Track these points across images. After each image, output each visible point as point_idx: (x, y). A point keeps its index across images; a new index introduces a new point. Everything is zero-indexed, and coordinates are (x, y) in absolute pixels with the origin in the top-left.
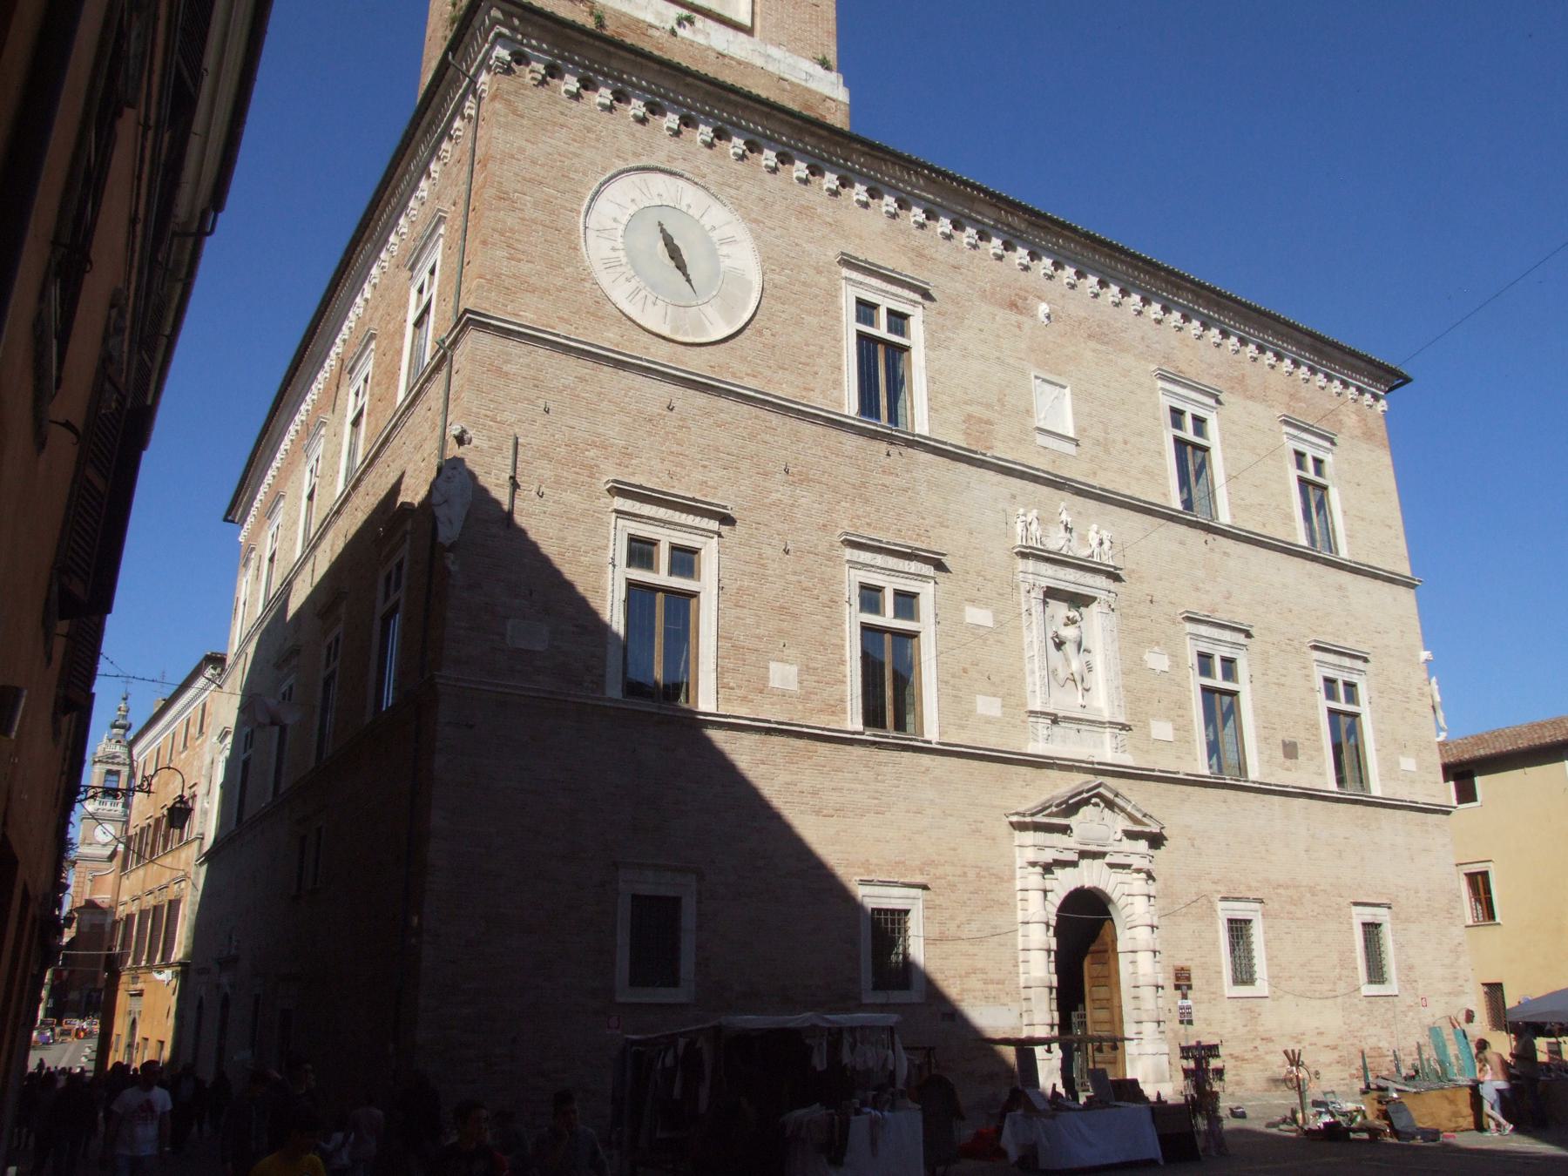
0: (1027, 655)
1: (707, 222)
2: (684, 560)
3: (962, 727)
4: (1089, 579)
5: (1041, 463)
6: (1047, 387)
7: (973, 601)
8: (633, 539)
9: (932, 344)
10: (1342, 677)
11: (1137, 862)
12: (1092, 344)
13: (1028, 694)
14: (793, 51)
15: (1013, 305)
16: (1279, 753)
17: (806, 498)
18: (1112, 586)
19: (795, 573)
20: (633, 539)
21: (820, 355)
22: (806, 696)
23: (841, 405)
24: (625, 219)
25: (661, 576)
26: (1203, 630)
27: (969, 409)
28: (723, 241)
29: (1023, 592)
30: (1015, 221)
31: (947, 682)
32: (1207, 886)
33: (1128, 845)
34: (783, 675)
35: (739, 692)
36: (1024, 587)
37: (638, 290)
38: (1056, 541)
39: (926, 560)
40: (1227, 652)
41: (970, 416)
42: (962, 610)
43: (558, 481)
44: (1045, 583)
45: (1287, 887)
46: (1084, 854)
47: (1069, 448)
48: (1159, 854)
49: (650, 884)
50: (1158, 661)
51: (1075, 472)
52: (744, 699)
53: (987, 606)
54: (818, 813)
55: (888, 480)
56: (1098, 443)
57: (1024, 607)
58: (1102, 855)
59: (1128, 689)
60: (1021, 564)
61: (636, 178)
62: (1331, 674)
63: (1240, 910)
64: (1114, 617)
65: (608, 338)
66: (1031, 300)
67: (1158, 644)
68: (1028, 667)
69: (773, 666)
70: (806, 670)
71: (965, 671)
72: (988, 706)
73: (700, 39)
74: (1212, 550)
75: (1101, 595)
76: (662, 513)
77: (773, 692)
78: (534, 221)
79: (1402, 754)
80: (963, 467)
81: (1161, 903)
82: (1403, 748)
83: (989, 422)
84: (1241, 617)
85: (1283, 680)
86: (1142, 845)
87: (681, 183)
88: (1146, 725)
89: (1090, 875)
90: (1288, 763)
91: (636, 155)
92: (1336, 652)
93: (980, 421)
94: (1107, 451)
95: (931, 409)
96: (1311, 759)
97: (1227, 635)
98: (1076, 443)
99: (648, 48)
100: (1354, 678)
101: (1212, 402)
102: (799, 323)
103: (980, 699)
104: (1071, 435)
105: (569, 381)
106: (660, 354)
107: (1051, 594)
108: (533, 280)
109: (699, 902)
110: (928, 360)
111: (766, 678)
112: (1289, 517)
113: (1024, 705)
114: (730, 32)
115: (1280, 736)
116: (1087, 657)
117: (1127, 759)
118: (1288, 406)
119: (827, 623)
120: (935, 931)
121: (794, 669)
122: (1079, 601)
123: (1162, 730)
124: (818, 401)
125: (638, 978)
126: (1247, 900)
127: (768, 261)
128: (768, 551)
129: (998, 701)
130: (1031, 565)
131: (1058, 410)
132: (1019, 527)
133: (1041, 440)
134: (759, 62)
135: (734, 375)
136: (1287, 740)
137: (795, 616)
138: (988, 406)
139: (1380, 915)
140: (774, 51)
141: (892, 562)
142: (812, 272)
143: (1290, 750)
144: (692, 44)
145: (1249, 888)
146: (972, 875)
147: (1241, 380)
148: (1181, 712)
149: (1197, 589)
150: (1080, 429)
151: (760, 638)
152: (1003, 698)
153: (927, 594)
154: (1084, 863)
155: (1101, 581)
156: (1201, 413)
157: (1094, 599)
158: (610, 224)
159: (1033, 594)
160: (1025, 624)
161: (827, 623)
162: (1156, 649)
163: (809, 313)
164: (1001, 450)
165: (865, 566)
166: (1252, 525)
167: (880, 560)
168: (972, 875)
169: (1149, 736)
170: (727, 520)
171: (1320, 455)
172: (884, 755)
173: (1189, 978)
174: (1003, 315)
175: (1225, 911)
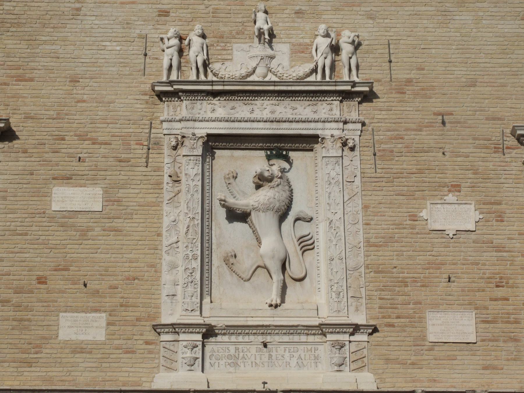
0: (167, 240)
7: (67, 179)
13: (164, 298)
18: (352, 110)
29: (166, 150)
36: (169, 142)
42: (48, 195)
50: (453, 216)
53: (94, 181)
57: (167, 171)
60: (166, 110)
64: (354, 162)
67: (456, 188)
71: (42, 280)
72: (81, 327)
88: (417, 320)
113: (157, 315)
116: (303, 229)
122: (280, 146)
129: (102, 318)
130: (183, 108)
148: (500, 292)
152: (110, 315)
157: (314, 139)
159: (183, 151)
160: (167, 196)
162: (451, 198)
169: (424, 338)
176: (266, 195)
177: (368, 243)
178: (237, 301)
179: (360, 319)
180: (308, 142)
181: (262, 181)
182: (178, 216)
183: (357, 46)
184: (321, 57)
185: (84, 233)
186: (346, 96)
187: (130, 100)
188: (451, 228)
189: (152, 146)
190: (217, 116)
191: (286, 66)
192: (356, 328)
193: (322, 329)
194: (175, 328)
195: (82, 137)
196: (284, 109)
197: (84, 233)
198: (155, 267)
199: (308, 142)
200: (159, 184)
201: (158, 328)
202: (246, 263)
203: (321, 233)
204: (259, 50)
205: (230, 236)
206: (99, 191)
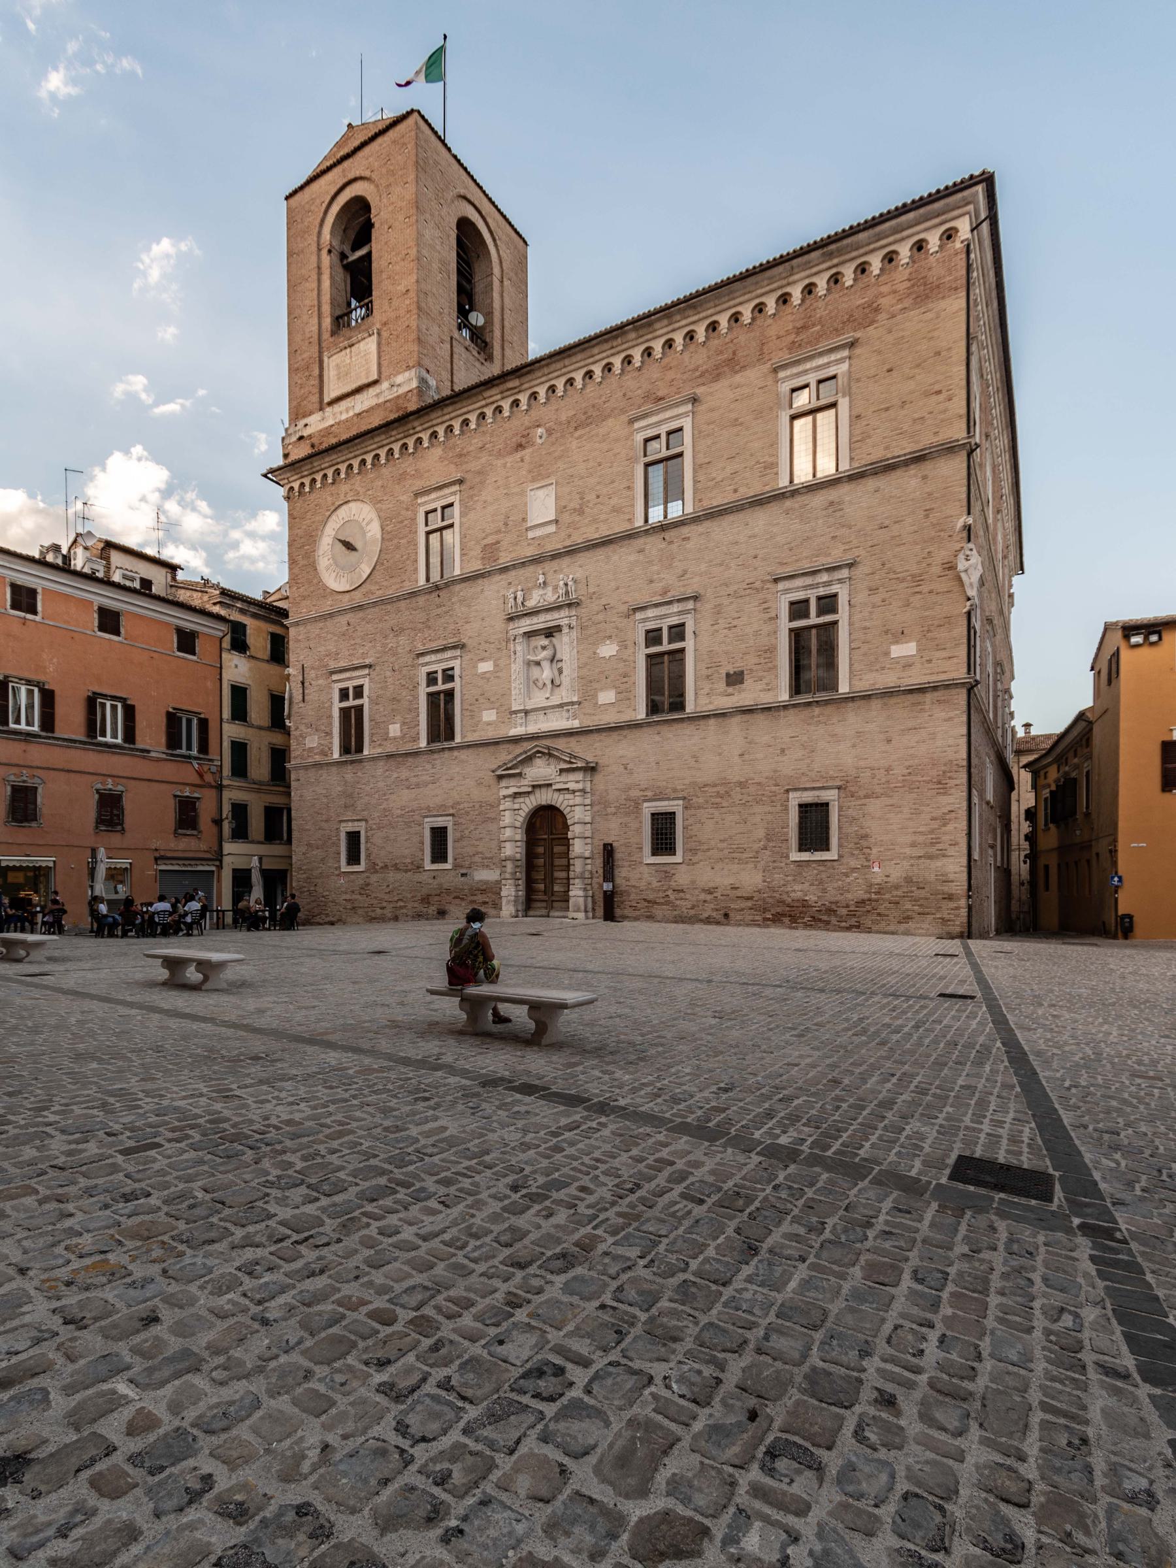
4: (556, 615)
5: (530, 552)
7: (482, 660)
11: (572, 786)
15: (520, 446)
16: (722, 685)
17: (403, 640)
22: (403, 737)
26: (650, 613)
32: (635, 793)
33: (564, 778)
34: (395, 730)
39: (454, 648)
40: (675, 621)
44: (522, 630)
45: (715, 785)
47: (552, 529)
48: (598, 778)
50: (608, 650)
55: (439, 611)
60: (511, 625)
61: (334, 517)
64: (574, 634)
72: (489, 716)
74: (671, 542)
76: (347, 675)
79: (897, 642)
80: (480, 581)
81: (596, 808)
82: (901, 636)
85: (735, 623)
88: (595, 696)
89: (543, 798)
90: (730, 690)
97: (675, 608)
100: (835, 589)
107: (529, 635)
117: (576, 724)
120: (458, 835)
122: (550, 633)
126: (669, 799)
130: (516, 624)
133: (531, 535)
141: (439, 656)
145: (675, 790)
149: (652, 581)
154: (537, 791)
164: (505, 559)
167: (433, 657)
170: (370, 666)
172: (436, 756)
175: (648, 808)
176: (545, 654)
178: (539, 699)
180: (558, 628)
181: (544, 648)
182: (517, 667)
183: (575, 581)
184: (561, 591)
186: (570, 605)
187: (500, 624)
188: (607, 655)
189: (508, 641)
190: (526, 625)
191: (550, 597)
192: (572, 703)
193: (561, 706)
194: (515, 712)
196: (549, 616)
199: (558, 628)
202: (540, 684)
203: (565, 666)
204: (541, 592)
205: (535, 672)
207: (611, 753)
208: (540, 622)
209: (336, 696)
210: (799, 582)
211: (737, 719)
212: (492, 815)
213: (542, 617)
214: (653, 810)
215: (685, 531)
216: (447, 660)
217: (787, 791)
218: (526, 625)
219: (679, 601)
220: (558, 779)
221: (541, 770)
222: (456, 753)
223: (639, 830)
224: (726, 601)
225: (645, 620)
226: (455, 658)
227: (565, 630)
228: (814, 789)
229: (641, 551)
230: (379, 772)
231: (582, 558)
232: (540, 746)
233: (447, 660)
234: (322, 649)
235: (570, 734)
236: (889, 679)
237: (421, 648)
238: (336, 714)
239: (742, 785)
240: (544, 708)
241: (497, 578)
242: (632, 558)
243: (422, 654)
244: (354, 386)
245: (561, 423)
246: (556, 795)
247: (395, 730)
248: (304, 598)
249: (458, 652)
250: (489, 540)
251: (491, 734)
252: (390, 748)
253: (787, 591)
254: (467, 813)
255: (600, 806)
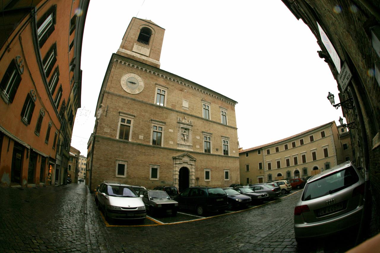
1: (138, 79)
2: (129, 122)
3: (167, 145)
4: (188, 126)
5: (183, 111)
6: (185, 101)
7: (170, 129)
8: (122, 119)
9: (168, 95)
10: (226, 140)
12: (192, 96)
14: (154, 59)
15: (181, 90)
16: (215, 150)
17: (147, 114)
19: (144, 124)
20: (122, 119)
21: (151, 96)
23: (154, 102)
24: (127, 79)
25: (126, 124)
26: (205, 134)
27: (173, 103)
28: (140, 81)
30: (182, 80)
31: (165, 139)
32: (203, 167)
33: (191, 162)
34: (141, 137)
35: (135, 139)
37: (127, 88)
38: (183, 121)
40: (209, 137)
41: (172, 104)
43: (113, 111)
44: (181, 126)
46: (184, 162)
47: (188, 109)
48: (196, 163)
49: (121, 163)
50: (198, 138)
51: (188, 112)
52: (135, 140)
53: (172, 129)
54: (145, 155)
56: (192, 108)
58: (187, 163)
59: (193, 141)
61: (129, 74)
62: (224, 140)
63: (208, 170)
65: (122, 93)
66: (184, 90)
67: (198, 135)
68: (178, 137)
69: (140, 136)
70: (144, 137)
72: (171, 142)
73: (141, 58)
75: (190, 129)
76: (126, 116)
77: (139, 139)
78: (115, 79)
82: (234, 150)
83: (175, 105)
84: (211, 132)
86: (193, 162)
87: (135, 74)
88: (196, 146)
89: (185, 165)
90: (217, 151)
91: (130, 71)
92: (225, 137)
93: (174, 105)
94: (193, 110)
95: (167, 103)
96: (220, 151)
97: (209, 135)
98: (188, 108)
99: (135, 59)
100: (228, 141)
101: (210, 104)
102: (149, 92)
103: (170, 141)
104: (188, 107)
105: (116, 99)
106: (128, 96)
107: (182, 128)
108: (114, 86)
109: (127, 165)
110: (167, 97)
111: (139, 137)
112: (220, 119)
114: (145, 57)
115: (216, 148)
116: (187, 137)
117: (192, 150)
118: (221, 105)
119: (148, 130)
121: (143, 136)
123: (198, 147)
124: (150, 102)
125: (119, 174)
127: (146, 84)
128: (140, 121)
129: (173, 142)
131: (186, 104)
132: (179, 119)
133: (183, 108)
134: (148, 60)
135: (139, 98)
136: (217, 148)
137: (144, 130)
138: (176, 103)
139: (228, 171)
140: (151, 59)
141: (158, 123)
142: (152, 85)
143: (217, 150)
144: (140, 58)
146: (167, 164)
147: (215, 102)
149: (205, 128)
150: (189, 107)
151: (138, 132)
153: (163, 127)
155: (190, 127)
156: (208, 105)
158: (125, 79)
161: (148, 130)
163: (151, 90)
164: (177, 109)
165: (154, 123)
166: (214, 120)
167: (157, 123)
168: (167, 164)
170: (135, 116)
171: (225, 112)
172: (155, 148)
173: (199, 179)
174: (179, 92)
175: (205, 170)
177: (193, 139)
179: (192, 145)
185: (172, 134)
190: (182, 126)
192: (192, 146)
194: (179, 144)
195: (172, 125)
197: (172, 134)
198: (177, 138)
200: (177, 131)
201: (177, 144)
206: (173, 130)
207: (198, 158)
208: (185, 126)
209: (120, 120)
210: (224, 138)
211: (218, 157)
212: (171, 167)
213: (186, 126)
214: (206, 171)
215: (210, 122)
216: (161, 125)
217: (224, 169)
218: (182, 126)
219: (210, 134)
220: (189, 162)
221: (186, 159)
222: (161, 150)
223: (203, 174)
224: (216, 137)
225: (204, 135)
226: (163, 125)
227: (190, 130)
228: (226, 169)
229: (203, 122)
230: (134, 148)
231: (193, 118)
232: (188, 154)
233: (161, 125)
234: (117, 104)
235: (191, 152)
236: (233, 155)
237: (152, 118)
238: (119, 125)
239: (218, 168)
240: (185, 145)
241: (175, 112)
242: (202, 123)
243: (154, 121)
244: (140, 53)
245: (189, 92)
246: (188, 165)
247: (141, 137)
248: (113, 87)
249: (164, 124)
250: (173, 103)
251: (171, 147)
252: (139, 142)
253: (223, 139)
254: (164, 166)
255: (197, 169)
